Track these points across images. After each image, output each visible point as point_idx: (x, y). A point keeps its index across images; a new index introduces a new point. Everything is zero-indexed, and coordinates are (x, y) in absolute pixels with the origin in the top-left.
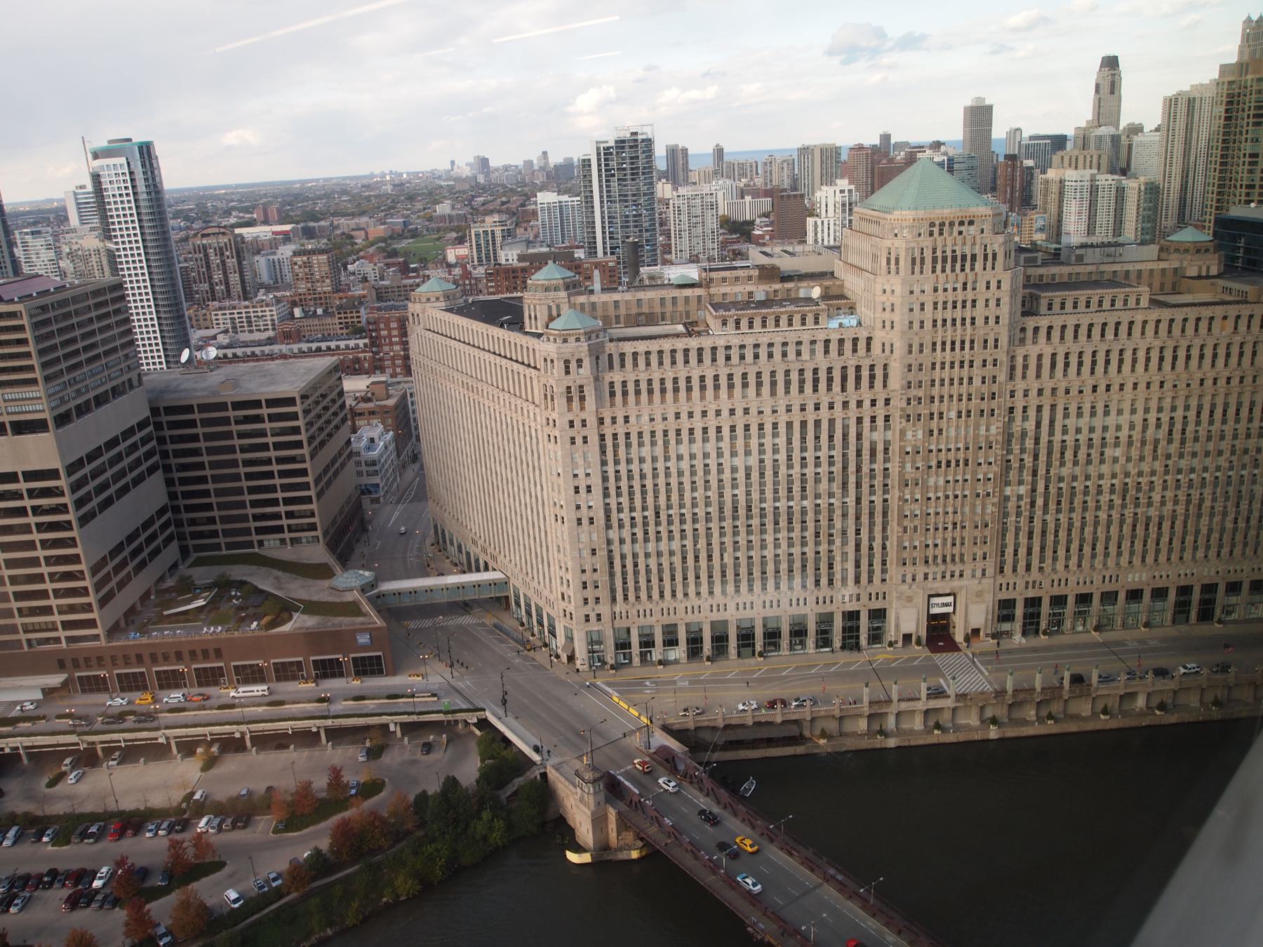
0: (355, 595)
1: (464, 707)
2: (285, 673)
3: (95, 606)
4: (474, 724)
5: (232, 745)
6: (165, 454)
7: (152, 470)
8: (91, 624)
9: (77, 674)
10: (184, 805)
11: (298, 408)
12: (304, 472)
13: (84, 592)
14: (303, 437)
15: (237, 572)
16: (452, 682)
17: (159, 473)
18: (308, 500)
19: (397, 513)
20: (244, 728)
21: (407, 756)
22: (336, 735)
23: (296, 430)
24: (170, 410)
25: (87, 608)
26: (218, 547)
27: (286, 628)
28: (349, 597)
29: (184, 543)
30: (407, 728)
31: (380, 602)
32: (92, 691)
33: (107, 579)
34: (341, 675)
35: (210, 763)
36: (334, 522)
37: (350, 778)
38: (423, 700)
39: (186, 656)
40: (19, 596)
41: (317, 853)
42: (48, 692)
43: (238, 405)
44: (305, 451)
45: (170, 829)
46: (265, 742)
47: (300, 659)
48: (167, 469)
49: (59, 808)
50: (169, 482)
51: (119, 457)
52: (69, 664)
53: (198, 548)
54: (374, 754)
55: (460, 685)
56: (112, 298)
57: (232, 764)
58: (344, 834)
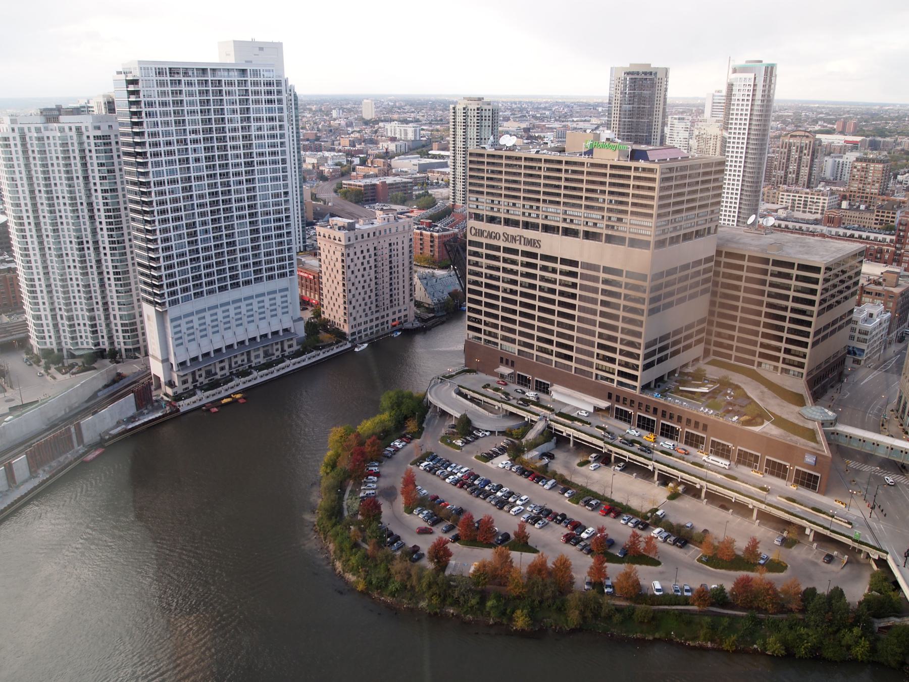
0: (816, 426)
1: (871, 543)
2: (745, 459)
3: (640, 368)
4: (874, 560)
5: (692, 491)
6: (716, 284)
7: (704, 292)
8: (634, 378)
9: (616, 406)
10: (649, 514)
11: (820, 276)
12: (809, 324)
13: (637, 357)
14: (817, 298)
15: (737, 378)
16: (869, 520)
17: (707, 297)
18: (805, 345)
19: (871, 377)
20: (704, 483)
21: (810, 557)
22: (764, 517)
23: (813, 292)
24: (729, 255)
25: (635, 367)
26: (729, 357)
27: (757, 429)
28: (810, 425)
29: (708, 347)
30: (819, 537)
31: (833, 439)
32: (621, 419)
33: (653, 353)
34: (784, 478)
35: (674, 496)
36: (819, 367)
37: (762, 551)
38: (839, 524)
39: (684, 421)
40: (601, 346)
41: (721, 590)
42: (597, 410)
44: (815, 309)
45: (636, 525)
46: (712, 497)
47: (759, 454)
48: (714, 294)
49: (579, 481)
50: (713, 303)
51: (686, 278)
52: (614, 397)
53: (716, 353)
54: (787, 543)
55: (874, 525)
56: (714, 171)
57: (687, 503)
58: (743, 584)
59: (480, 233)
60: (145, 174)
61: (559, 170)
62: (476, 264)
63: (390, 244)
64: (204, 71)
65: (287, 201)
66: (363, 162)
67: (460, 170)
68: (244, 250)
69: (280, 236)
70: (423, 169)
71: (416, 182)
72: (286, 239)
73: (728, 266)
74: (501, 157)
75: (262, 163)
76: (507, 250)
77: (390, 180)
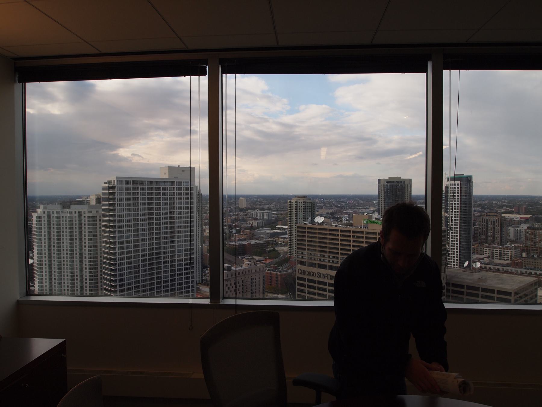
43: (484, 290)
59: (304, 272)
60: (114, 238)
61: (349, 236)
62: (302, 291)
63: (252, 279)
64: (151, 182)
66: (238, 232)
67: (293, 236)
68: (166, 282)
70: (272, 235)
71: (268, 243)
73: (454, 292)
74: (315, 229)
75: (180, 232)
76: (320, 283)
77: (253, 242)
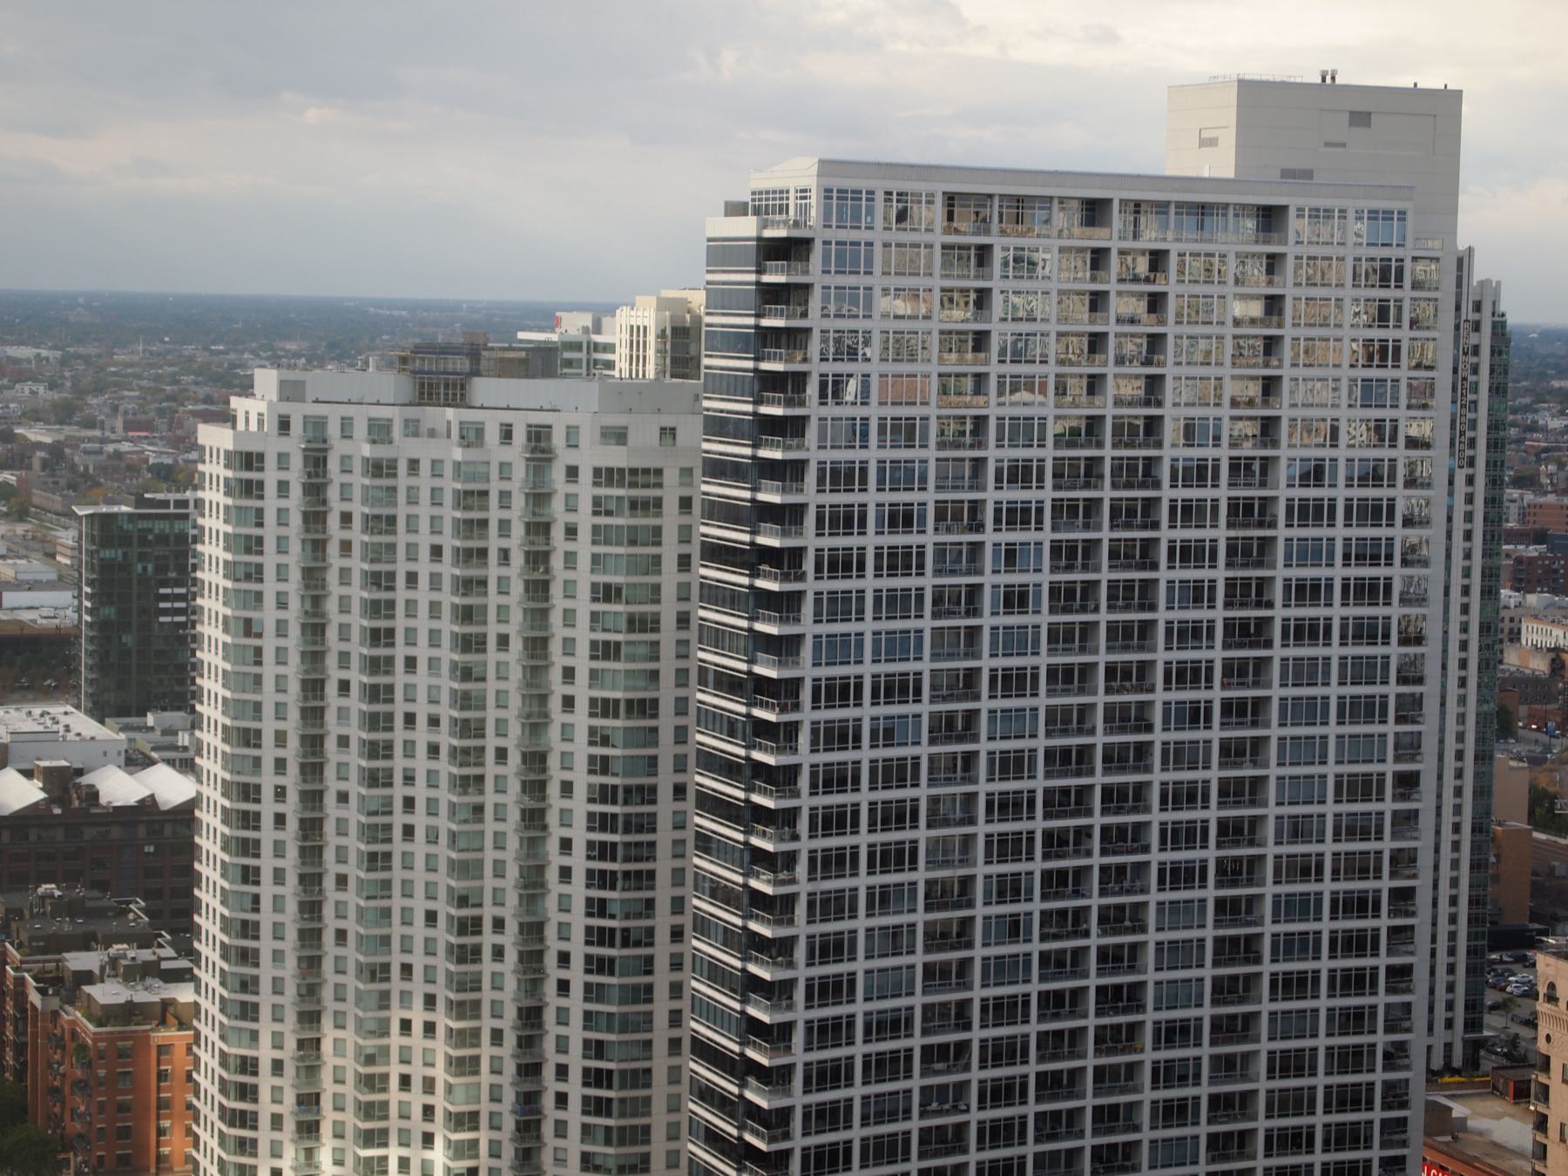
60: (784, 647)
64: (1094, 211)
65: (1401, 935)
68: (1173, 1034)
69: (1356, 982)
72: (1382, 999)
